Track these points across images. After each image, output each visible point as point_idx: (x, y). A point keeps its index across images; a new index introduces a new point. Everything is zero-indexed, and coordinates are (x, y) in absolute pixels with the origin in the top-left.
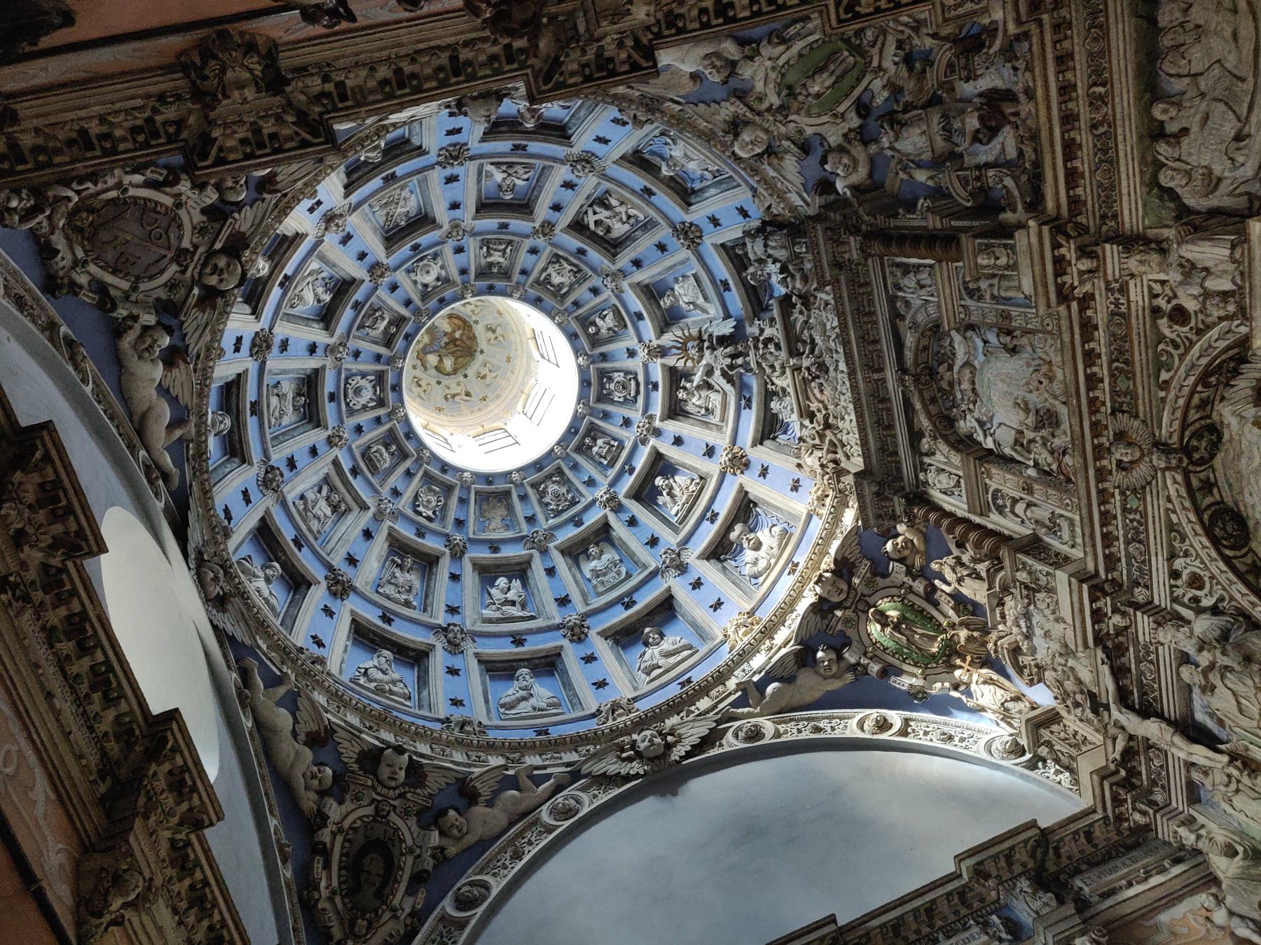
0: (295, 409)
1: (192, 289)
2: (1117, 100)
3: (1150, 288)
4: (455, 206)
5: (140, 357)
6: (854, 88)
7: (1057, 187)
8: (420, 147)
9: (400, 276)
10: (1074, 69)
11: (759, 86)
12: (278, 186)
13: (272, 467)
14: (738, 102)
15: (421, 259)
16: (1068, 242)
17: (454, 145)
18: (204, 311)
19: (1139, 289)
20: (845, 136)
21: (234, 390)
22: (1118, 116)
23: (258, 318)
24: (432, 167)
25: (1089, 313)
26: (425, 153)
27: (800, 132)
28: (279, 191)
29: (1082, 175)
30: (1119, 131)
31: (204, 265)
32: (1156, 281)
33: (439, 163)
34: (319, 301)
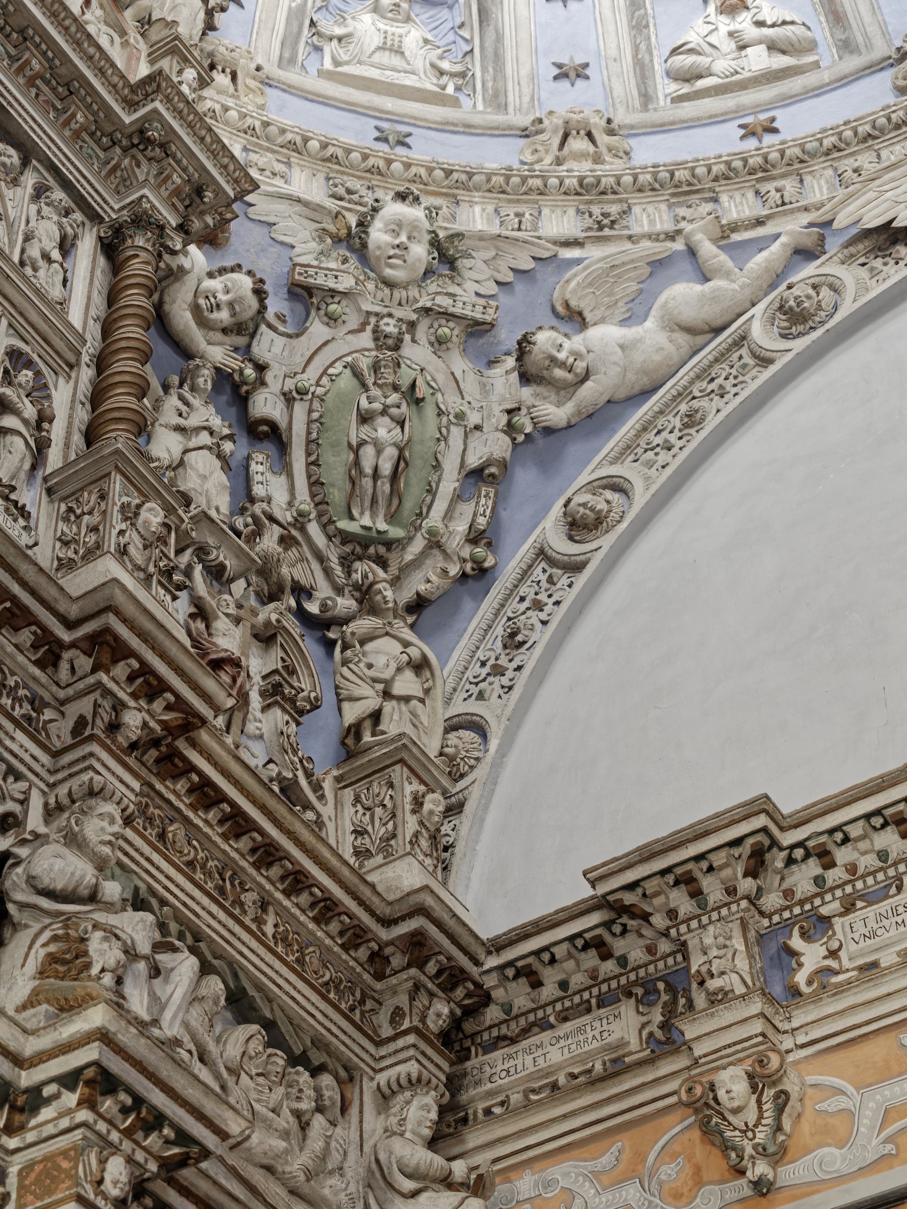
2: (254, 944)
3: (18, 777)
6: (313, 464)
7: (215, 765)
10: (303, 911)
11: (460, 364)
14: (478, 316)
16: (160, 722)
19: (27, 758)
20: (261, 368)
22: (237, 929)
25: (26, 636)
27: (332, 320)
29: (193, 807)
30: (222, 916)
32: (27, 793)
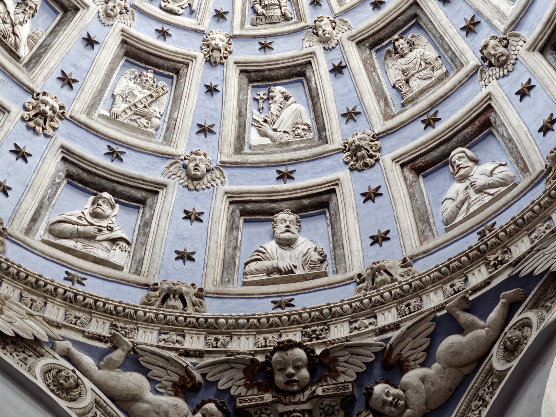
0: (412, 45)
1: (318, 396)
4: (90, 42)
5: (406, 406)
8: (64, 159)
9: (207, 23)
12: (182, 373)
13: (484, 59)
15: (171, 12)
17: (34, 129)
18: (335, 359)
21: (420, 162)
23: (337, 182)
24: (73, 120)
26: (65, 149)
28: (186, 369)
31: (294, 393)
33: (62, 117)
34: (286, 98)
